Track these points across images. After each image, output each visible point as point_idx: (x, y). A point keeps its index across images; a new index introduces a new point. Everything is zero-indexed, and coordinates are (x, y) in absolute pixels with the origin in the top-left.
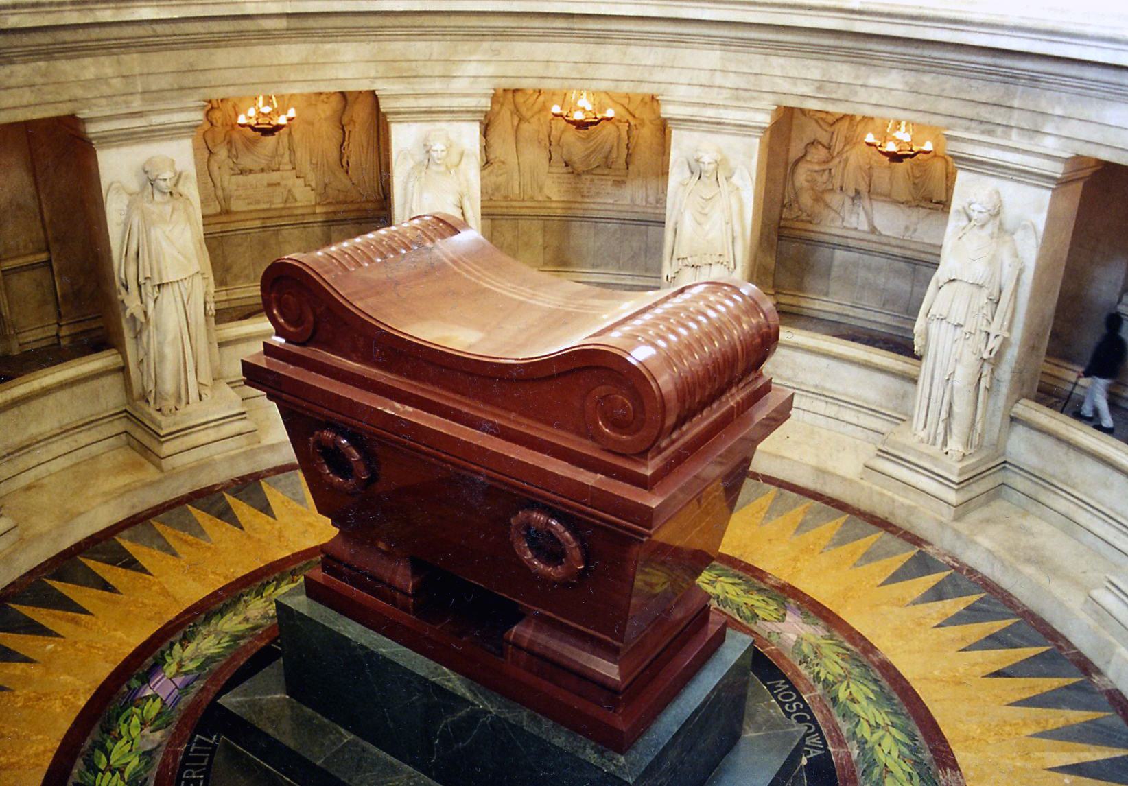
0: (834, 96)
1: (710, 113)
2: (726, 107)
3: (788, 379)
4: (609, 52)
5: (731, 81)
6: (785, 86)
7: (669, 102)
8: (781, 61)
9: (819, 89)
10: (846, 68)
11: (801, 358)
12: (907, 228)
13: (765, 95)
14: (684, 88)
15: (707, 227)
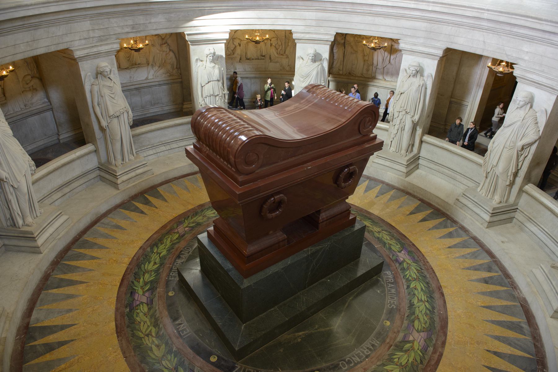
0: (139, 30)
1: (95, 50)
2: (101, 45)
3: (148, 145)
4: (40, 32)
5: (97, 34)
6: (119, 30)
7: (77, 50)
8: (115, 20)
9: (133, 28)
10: (141, 17)
11: (149, 135)
12: (131, 77)
13: (112, 36)
14: (78, 42)
15: (116, 98)
